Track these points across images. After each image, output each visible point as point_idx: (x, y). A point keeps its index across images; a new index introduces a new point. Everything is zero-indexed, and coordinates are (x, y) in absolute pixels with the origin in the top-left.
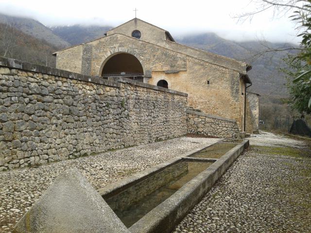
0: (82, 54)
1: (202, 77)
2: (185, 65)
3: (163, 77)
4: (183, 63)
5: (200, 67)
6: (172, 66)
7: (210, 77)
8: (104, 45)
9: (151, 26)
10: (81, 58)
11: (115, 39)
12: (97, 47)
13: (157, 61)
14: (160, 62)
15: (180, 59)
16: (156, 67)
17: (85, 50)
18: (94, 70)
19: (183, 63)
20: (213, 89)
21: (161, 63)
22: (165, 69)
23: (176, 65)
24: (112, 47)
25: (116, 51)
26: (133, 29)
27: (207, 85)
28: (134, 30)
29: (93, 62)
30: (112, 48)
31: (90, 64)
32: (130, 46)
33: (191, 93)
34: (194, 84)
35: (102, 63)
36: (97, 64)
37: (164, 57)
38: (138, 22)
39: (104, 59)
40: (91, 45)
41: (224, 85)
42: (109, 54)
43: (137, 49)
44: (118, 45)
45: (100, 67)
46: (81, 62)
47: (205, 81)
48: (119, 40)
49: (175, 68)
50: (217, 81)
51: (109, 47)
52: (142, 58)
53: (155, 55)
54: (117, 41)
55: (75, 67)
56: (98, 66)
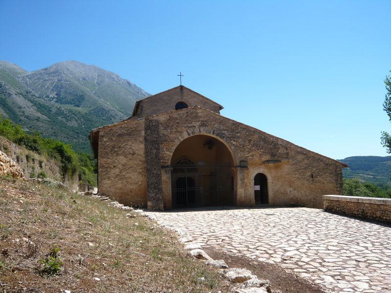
0: (143, 133)
1: (305, 169)
2: (287, 154)
3: (262, 170)
4: (285, 151)
5: (303, 157)
6: (273, 155)
7: (314, 169)
8: (178, 123)
9: (202, 98)
10: (142, 139)
11: (194, 115)
12: (167, 126)
13: (254, 148)
14: (258, 150)
15: (281, 147)
16: (252, 156)
17: (147, 128)
18: (163, 158)
19: (285, 151)
20: (318, 184)
21: (258, 151)
22: (264, 158)
23: (278, 153)
24: (189, 125)
25: (197, 133)
26: (177, 99)
27: (311, 179)
28: (180, 100)
29: (161, 146)
30: (191, 127)
31: (158, 149)
32: (216, 126)
33: (295, 190)
34: (298, 178)
35: (174, 148)
36: (168, 150)
37: (262, 143)
38: (184, 91)
39: (177, 143)
40: (157, 121)
41: (328, 179)
42: (186, 136)
43: (226, 130)
44: (198, 124)
45: (172, 154)
46: (142, 146)
47: (309, 174)
48: (200, 117)
49: (276, 158)
50: (321, 174)
51: (185, 125)
52: (235, 143)
53: (251, 140)
54: (196, 117)
55: (133, 154)
56: (168, 153)
